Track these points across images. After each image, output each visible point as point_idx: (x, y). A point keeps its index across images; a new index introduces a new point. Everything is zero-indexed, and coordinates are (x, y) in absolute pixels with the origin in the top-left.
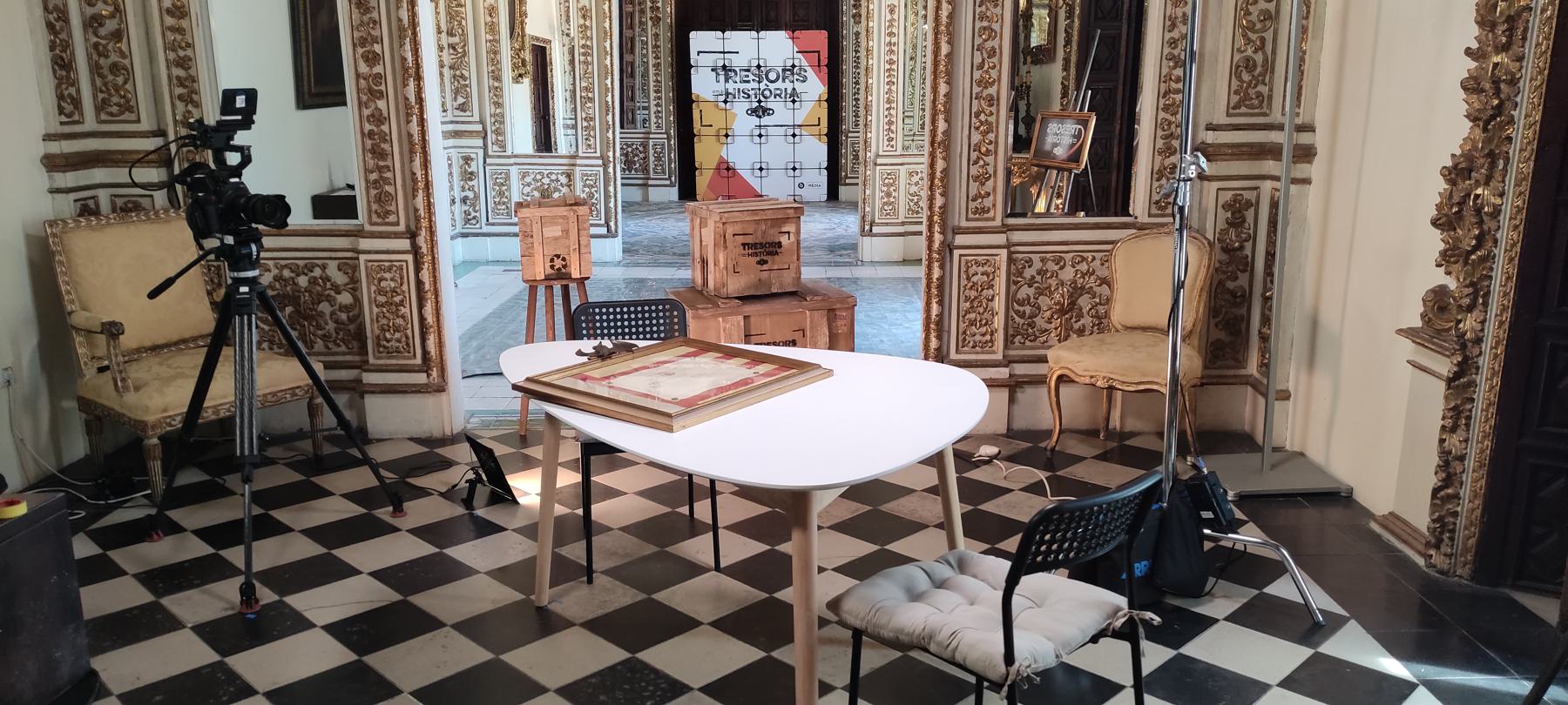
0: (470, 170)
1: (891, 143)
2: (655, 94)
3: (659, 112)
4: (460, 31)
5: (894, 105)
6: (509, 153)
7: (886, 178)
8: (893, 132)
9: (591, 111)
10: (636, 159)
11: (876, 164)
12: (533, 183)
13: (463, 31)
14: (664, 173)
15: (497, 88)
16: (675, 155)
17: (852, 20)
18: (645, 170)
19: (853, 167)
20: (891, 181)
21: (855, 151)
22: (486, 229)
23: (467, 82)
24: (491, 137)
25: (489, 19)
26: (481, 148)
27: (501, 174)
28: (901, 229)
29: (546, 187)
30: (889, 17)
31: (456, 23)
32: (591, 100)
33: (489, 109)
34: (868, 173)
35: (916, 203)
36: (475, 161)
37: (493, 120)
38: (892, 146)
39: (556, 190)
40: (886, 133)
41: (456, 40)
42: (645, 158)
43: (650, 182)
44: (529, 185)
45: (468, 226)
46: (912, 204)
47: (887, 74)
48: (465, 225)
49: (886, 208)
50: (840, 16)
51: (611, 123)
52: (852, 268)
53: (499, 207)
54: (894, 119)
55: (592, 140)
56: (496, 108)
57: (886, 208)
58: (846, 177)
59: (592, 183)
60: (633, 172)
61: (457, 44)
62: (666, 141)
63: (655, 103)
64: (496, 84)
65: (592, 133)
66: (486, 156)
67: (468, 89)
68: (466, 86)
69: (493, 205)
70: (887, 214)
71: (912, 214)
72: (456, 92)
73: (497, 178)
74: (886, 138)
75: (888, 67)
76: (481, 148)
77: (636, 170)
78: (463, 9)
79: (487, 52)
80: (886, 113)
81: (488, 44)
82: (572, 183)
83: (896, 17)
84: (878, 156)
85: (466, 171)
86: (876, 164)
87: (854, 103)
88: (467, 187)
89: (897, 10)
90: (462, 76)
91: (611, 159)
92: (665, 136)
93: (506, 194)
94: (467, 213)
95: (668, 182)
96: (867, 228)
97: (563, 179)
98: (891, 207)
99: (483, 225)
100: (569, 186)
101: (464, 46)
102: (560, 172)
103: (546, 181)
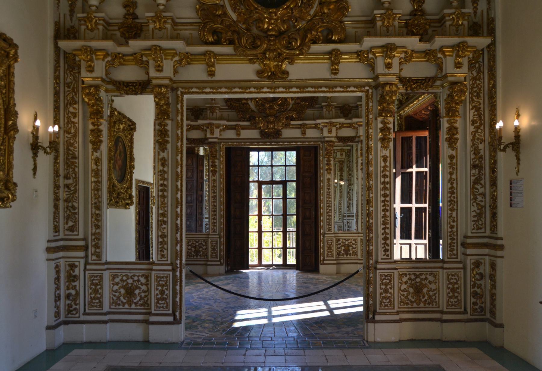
0: (73, 274)
1: (387, 253)
2: (213, 213)
3: (215, 223)
4: (73, 175)
5: (388, 226)
6: (104, 261)
7: (384, 279)
8: (388, 245)
9: (165, 231)
10: (201, 249)
11: (376, 269)
12: (121, 283)
13: (76, 175)
14: (216, 257)
15: (98, 214)
16: (223, 247)
17: (326, 172)
18: (206, 255)
20: (388, 281)
21: (329, 245)
22: (83, 318)
23: (76, 211)
24: (91, 250)
25: (94, 167)
26: (82, 258)
27: (96, 276)
28: (396, 317)
29: (130, 285)
30: (383, 164)
31: (71, 170)
32: (165, 223)
33: (91, 230)
34: (371, 275)
35: (406, 297)
36: (78, 268)
37: (93, 237)
38: (388, 256)
39: (137, 288)
40: (382, 246)
41: (70, 181)
42: (206, 249)
43: (209, 263)
44: (117, 284)
45: (70, 315)
46: (403, 297)
47: (383, 204)
48: (68, 314)
49: (384, 301)
50: (319, 170)
51: (179, 239)
52: (365, 351)
53: (94, 301)
54: (388, 236)
55: (165, 252)
56: (96, 229)
57: (384, 301)
58: (324, 260)
59: (163, 283)
60: (199, 257)
61: (71, 184)
62: (218, 239)
63: (213, 217)
64: (97, 212)
65: (165, 246)
66: (87, 263)
67: (77, 216)
68: (75, 213)
69: (90, 300)
70: (385, 306)
71: (403, 305)
72: (68, 218)
73: (94, 280)
74: (383, 250)
75: (383, 199)
76: (82, 258)
77: (200, 256)
78: (77, 161)
79: (92, 190)
80: (383, 231)
81: (93, 184)
82: (149, 283)
83: (388, 164)
84: (377, 262)
85: (70, 274)
86: (376, 269)
87: (328, 217)
88: (71, 287)
89: (388, 159)
90: (74, 207)
91: (178, 266)
92: (218, 236)
93: (100, 291)
94: (70, 306)
95: (219, 263)
96: (371, 316)
97: (143, 280)
98: (388, 301)
99: (81, 314)
100: (147, 285)
101: (76, 185)
102: (141, 274)
103: (130, 281)
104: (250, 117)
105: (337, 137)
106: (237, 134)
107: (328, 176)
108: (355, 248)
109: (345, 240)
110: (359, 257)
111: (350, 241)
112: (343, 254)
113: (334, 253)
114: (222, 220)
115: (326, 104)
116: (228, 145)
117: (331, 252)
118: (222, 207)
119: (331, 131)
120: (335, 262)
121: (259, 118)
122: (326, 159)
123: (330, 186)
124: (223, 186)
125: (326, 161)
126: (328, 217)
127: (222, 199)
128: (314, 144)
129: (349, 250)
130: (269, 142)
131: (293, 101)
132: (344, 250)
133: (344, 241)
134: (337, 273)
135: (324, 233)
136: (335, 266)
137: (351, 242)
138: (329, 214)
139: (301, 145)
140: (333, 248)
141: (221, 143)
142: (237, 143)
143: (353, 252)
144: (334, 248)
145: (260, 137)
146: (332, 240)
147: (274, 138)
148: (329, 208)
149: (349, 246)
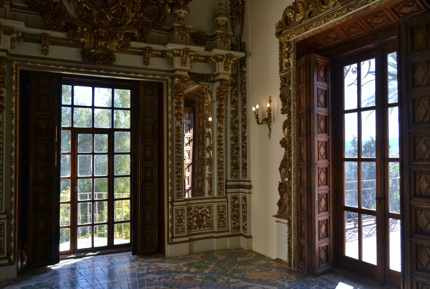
16: (15, 234)
19: (177, 229)
21: (178, 216)
62: (5, 221)
87: (177, 179)
92: (5, 216)
104: (67, 24)
105: (189, 73)
106: (43, 50)
107: (178, 124)
108: (209, 218)
109: (198, 208)
110: (215, 229)
111: (203, 209)
112: (195, 227)
113: (186, 226)
114: (13, 189)
115: (179, 25)
116: (27, 66)
117: (182, 226)
118: (13, 167)
119: (185, 63)
120: (187, 239)
121: (82, 29)
122: (175, 100)
123: (180, 137)
124: (16, 132)
125: (176, 103)
126: (177, 179)
127: (13, 154)
128: (160, 79)
129: (202, 221)
130: (96, 69)
131: (134, 14)
132: (197, 222)
133: (197, 209)
134: (190, 254)
135: (173, 201)
136: (187, 244)
137: (205, 210)
138: (178, 174)
139: (142, 78)
140: (183, 220)
141: (13, 61)
142: (41, 64)
143: (207, 223)
144: (185, 221)
145: (82, 61)
146: (182, 210)
147: (103, 64)
148: (179, 167)
149: (203, 215)
